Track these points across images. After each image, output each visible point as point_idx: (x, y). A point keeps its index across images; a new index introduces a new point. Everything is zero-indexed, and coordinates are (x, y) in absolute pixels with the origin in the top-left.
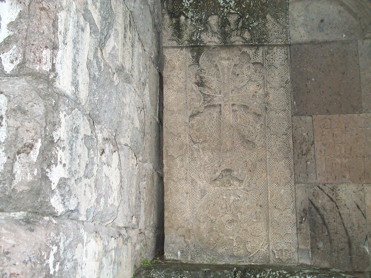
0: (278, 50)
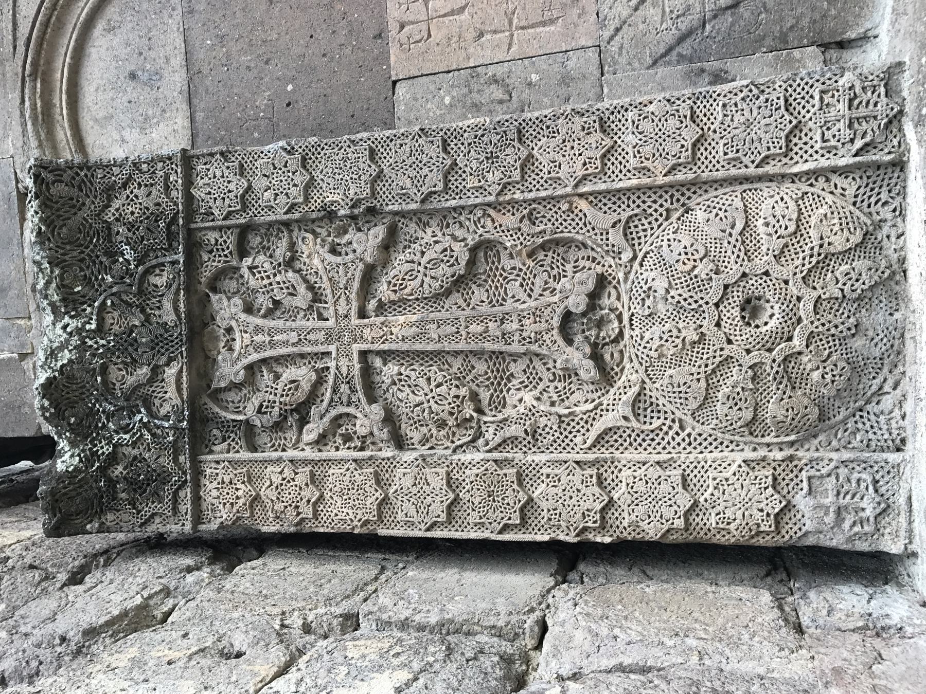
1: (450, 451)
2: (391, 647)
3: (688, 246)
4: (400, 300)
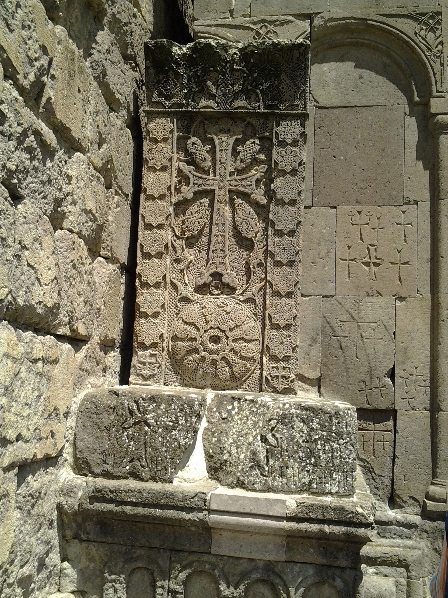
1: (172, 226)
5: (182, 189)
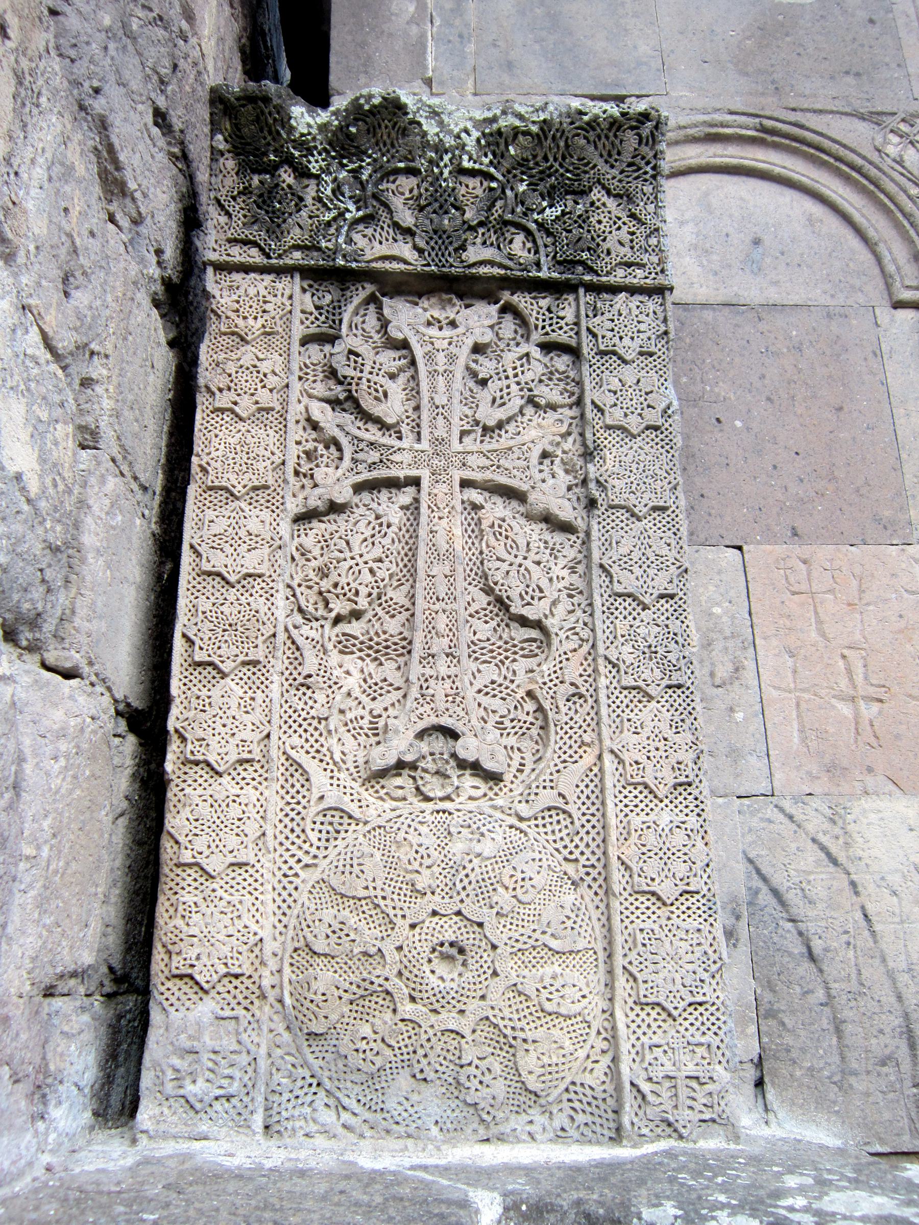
0: (633, 306)
1: (288, 581)
2: (64, 479)
3: (532, 882)
4: (481, 531)
5: (319, 474)
